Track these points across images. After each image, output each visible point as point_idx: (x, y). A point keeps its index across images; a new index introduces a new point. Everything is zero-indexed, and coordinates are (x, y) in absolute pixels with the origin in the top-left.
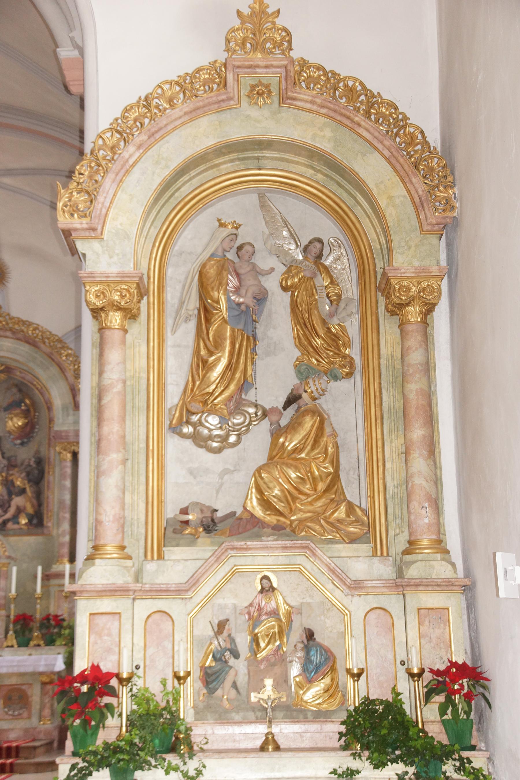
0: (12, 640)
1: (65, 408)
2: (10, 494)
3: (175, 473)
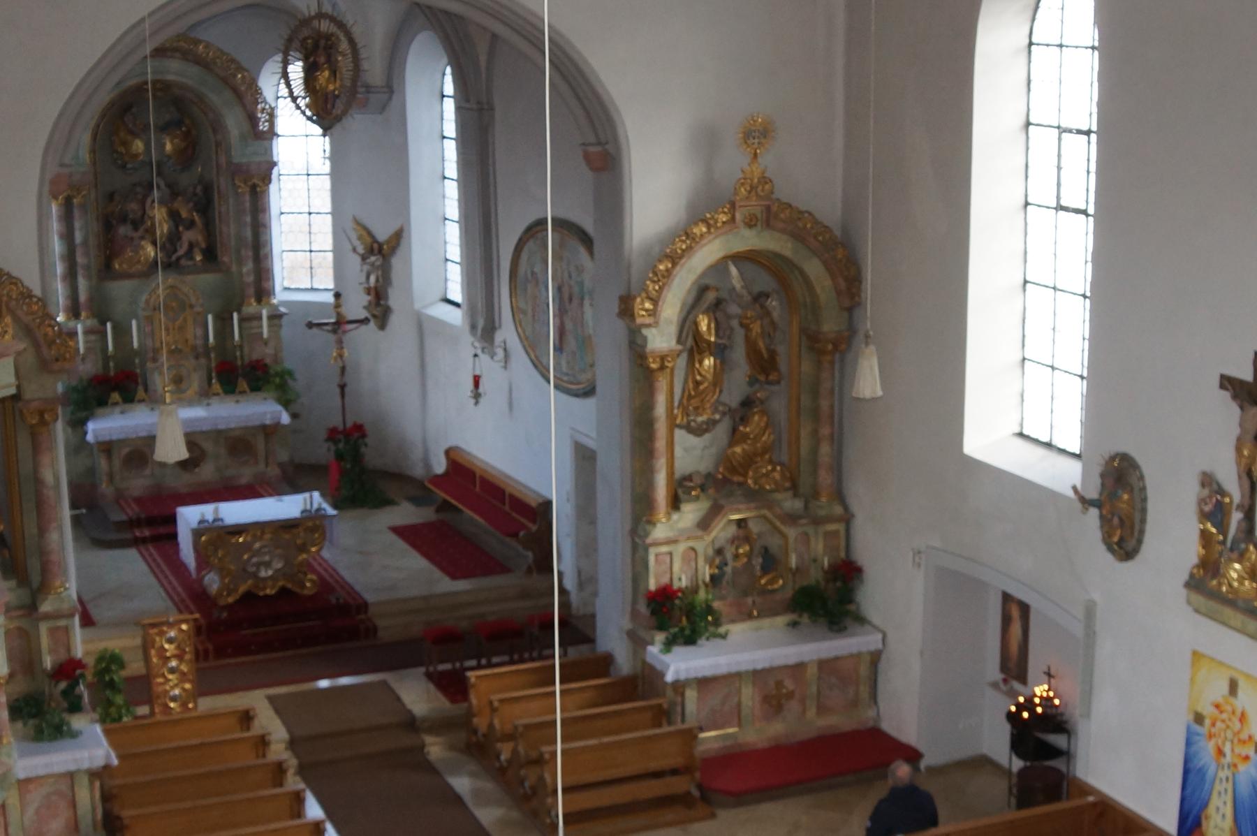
0: (216, 387)
1: (243, 138)
2: (177, 227)
3: (678, 451)
